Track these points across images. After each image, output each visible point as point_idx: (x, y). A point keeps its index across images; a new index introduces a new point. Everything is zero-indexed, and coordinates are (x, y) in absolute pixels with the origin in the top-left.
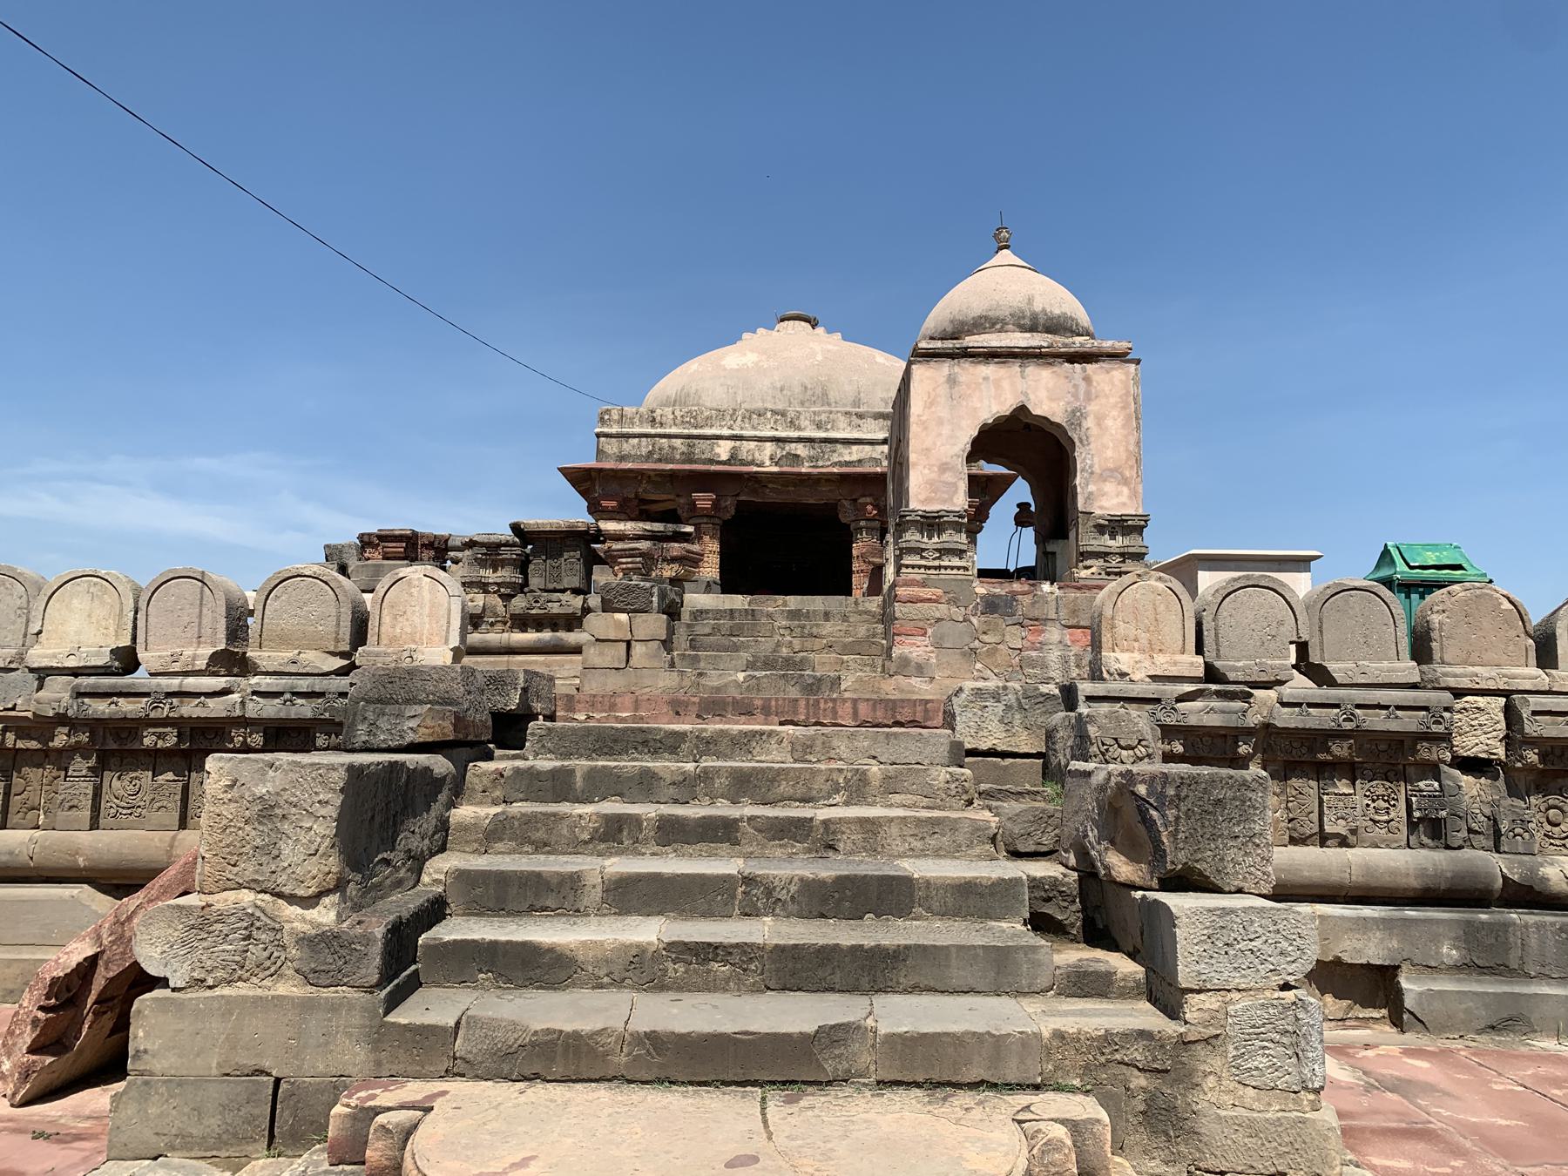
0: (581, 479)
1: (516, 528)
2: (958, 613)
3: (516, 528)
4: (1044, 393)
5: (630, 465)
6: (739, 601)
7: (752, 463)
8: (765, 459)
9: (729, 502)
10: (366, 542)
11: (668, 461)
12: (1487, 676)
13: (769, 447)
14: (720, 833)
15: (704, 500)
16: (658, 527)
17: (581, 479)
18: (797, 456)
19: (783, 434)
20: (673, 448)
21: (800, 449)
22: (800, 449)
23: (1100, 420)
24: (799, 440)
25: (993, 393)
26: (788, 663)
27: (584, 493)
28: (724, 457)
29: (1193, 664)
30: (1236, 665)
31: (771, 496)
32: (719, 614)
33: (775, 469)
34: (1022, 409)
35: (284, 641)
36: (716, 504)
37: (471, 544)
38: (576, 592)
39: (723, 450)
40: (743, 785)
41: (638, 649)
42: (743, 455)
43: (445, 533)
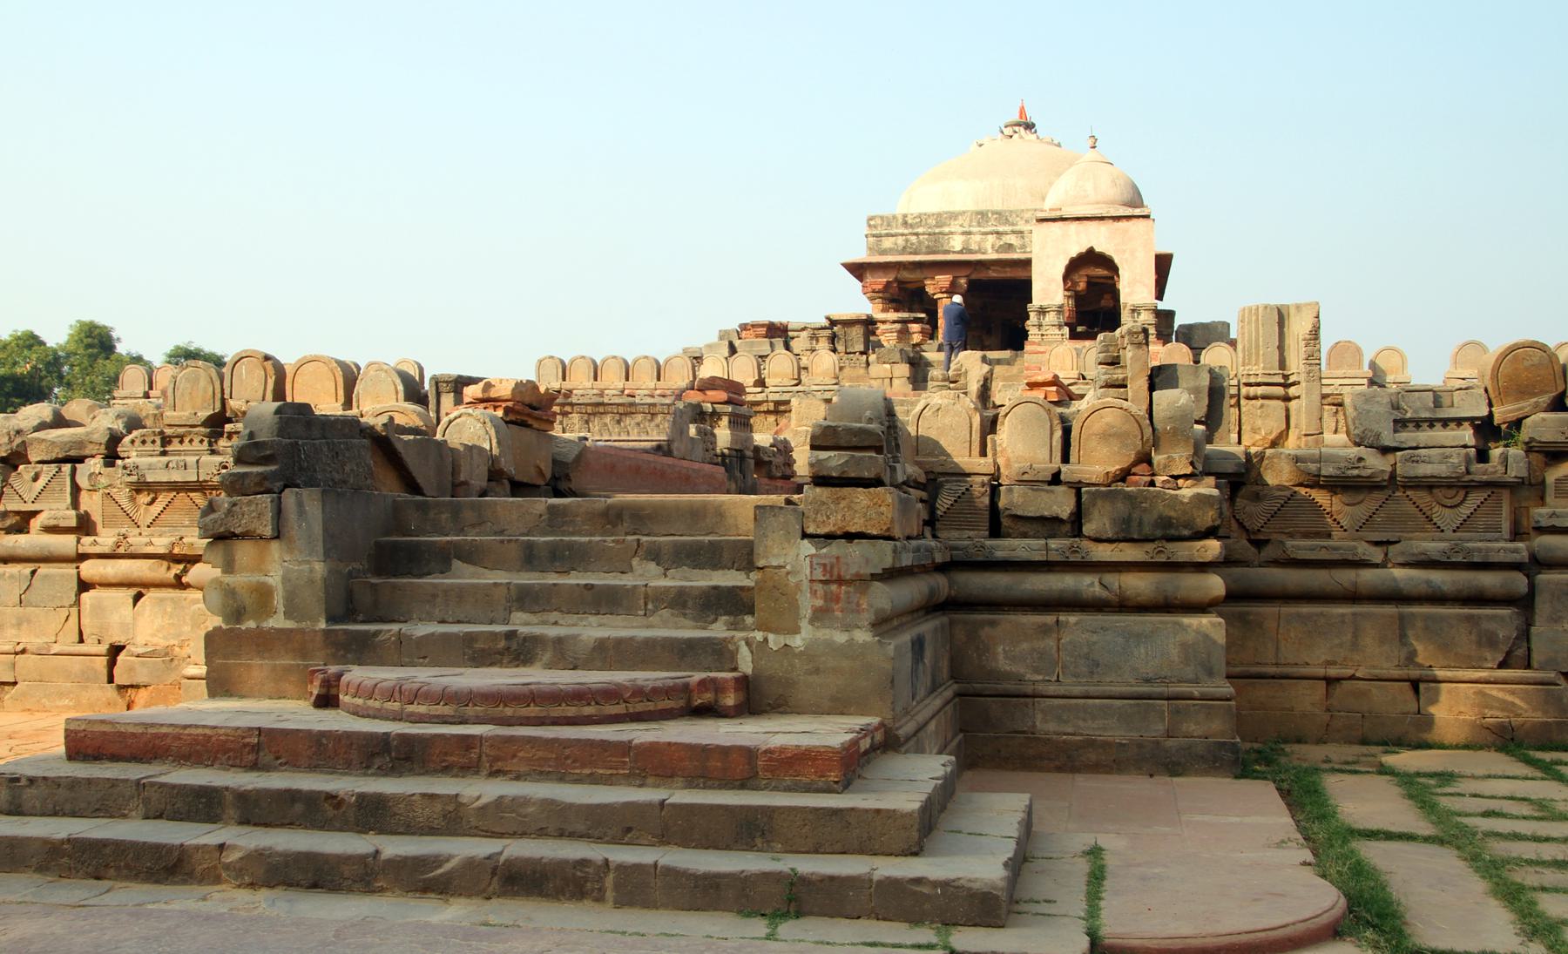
0: (858, 270)
3: (828, 318)
4: (1100, 239)
7: (979, 251)
8: (989, 251)
10: (744, 327)
11: (915, 253)
13: (991, 238)
15: (944, 280)
16: (905, 315)
18: (1010, 245)
19: (1001, 229)
20: (920, 242)
22: (1012, 239)
24: (1013, 232)
25: (1077, 240)
27: (860, 278)
28: (958, 248)
31: (993, 274)
33: (995, 256)
34: (1091, 251)
35: (776, 375)
37: (803, 329)
38: (862, 353)
39: (957, 243)
41: (895, 382)
42: (974, 247)
43: (784, 320)
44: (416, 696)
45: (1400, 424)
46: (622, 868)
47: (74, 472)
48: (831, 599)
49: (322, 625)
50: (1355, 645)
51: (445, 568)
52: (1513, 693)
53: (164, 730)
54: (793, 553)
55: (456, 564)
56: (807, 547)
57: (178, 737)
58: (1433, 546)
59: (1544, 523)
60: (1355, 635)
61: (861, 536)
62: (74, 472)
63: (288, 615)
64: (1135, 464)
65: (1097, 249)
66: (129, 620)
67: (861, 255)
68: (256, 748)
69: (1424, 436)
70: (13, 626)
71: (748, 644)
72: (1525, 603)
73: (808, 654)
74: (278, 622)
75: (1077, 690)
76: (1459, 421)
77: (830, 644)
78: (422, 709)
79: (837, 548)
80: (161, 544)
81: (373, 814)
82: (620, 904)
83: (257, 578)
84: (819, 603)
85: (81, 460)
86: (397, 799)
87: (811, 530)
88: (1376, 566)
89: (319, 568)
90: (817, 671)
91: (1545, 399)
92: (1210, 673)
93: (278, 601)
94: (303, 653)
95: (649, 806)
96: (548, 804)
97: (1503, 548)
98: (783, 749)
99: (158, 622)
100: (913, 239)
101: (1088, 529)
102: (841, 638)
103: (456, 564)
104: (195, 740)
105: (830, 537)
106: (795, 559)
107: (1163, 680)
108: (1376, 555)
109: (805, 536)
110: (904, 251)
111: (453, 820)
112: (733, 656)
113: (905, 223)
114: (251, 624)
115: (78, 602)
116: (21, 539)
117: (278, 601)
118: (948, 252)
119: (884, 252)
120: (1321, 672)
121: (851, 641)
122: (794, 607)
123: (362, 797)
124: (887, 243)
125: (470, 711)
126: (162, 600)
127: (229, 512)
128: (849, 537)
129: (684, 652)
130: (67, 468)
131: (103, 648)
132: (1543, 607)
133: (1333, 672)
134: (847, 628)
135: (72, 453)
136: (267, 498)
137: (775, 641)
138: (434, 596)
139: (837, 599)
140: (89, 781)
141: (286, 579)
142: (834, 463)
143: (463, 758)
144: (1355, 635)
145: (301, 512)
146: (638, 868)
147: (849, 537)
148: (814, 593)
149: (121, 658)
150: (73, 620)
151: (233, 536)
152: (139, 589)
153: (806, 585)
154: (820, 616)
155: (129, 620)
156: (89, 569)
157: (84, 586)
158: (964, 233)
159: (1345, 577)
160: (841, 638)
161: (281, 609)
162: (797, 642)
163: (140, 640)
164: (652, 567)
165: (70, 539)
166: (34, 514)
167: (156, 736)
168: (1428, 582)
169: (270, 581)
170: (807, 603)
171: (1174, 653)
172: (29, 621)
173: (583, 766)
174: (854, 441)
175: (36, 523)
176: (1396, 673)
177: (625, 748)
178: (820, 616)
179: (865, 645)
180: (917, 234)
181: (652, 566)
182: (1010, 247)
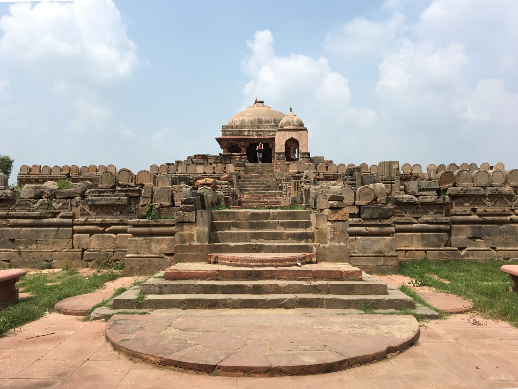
0: (219, 140)
1: (220, 154)
2: (283, 166)
3: (220, 154)
4: (294, 135)
5: (228, 137)
6: (253, 164)
9: (248, 144)
12: (322, 171)
13: (255, 133)
14: (258, 184)
15: (243, 143)
17: (219, 140)
21: (261, 133)
22: (261, 133)
23: (303, 139)
26: (261, 173)
27: (220, 143)
29: (297, 171)
30: (300, 171)
32: (250, 166)
33: (256, 137)
34: (292, 138)
36: (245, 144)
40: (259, 181)
44: (237, 260)
45: (420, 190)
46: (327, 299)
47: (71, 200)
48: (334, 235)
49: (207, 244)
50: (412, 242)
51: (229, 229)
52: (448, 253)
53: (193, 271)
54: (325, 225)
55: (232, 228)
56: (329, 224)
57: (197, 273)
58: (429, 218)
59: (453, 213)
60: (412, 240)
61: (341, 221)
62: (71, 200)
63: (198, 241)
64: (373, 201)
65: (294, 138)
66: (88, 242)
67: (220, 135)
68: (217, 275)
69: (425, 193)
70: (51, 244)
71: (315, 246)
72: (449, 232)
73: (330, 248)
74: (195, 243)
75: (361, 254)
76: (432, 190)
77: (335, 246)
78: (254, 264)
79: (336, 223)
80: (99, 220)
81: (257, 290)
82: (326, 308)
83: (189, 232)
84: (332, 236)
85: (73, 198)
86: (263, 285)
87: (330, 219)
88: (416, 223)
89: (207, 230)
90: (331, 252)
91: (451, 184)
92: (392, 250)
93: (195, 238)
94: (202, 251)
95: (325, 285)
96: (300, 285)
97: (443, 219)
98: (348, 271)
99: (97, 242)
100: (235, 132)
101: (363, 216)
102: (337, 244)
103: (232, 228)
104: (202, 274)
105: (334, 221)
106: (327, 226)
107: (381, 252)
108: (415, 221)
109: (328, 221)
110: (232, 135)
111: (277, 290)
112: (312, 249)
113: (232, 128)
114: (188, 244)
115: (72, 237)
116: (55, 220)
117: (195, 238)
118: (244, 136)
119: (227, 135)
120: (404, 248)
121: (339, 245)
122: (326, 238)
123: (254, 285)
124: (227, 133)
125: (266, 264)
126: (98, 236)
127: (183, 216)
128: (339, 221)
129: (300, 249)
130: (69, 200)
131: (80, 250)
132: (453, 232)
133: (407, 248)
134: (339, 242)
135: (71, 196)
136: (194, 212)
137: (321, 245)
138: (232, 236)
139: (336, 235)
140: (182, 285)
141: (197, 233)
142: (335, 204)
143: (271, 275)
144: (412, 240)
145: (202, 216)
146: (331, 299)
147: (339, 221)
148: (331, 234)
149: (85, 252)
150: (71, 242)
151: (184, 222)
152: (91, 233)
153: (329, 232)
154: (332, 239)
155: (88, 242)
156: (75, 227)
157: (74, 232)
158: (248, 131)
159: (409, 226)
160: (337, 244)
161: (196, 240)
162: (327, 246)
163: (91, 247)
164: (282, 228)
165: (70, 220)
166: (59, 213)
167: (191, 273)
168: (428, 227)
169: (193, 233)
170: (329, 236)
171: (383, 245)
172: (57, 243)
173: (301, 276)
174: (338, 199)
175: (60, 215)
176: (421, 248)
177: (310, 272)
178: (332, 239)
179: (343, 246)
180: (235, 131)
181: (282, 227)
182: (260, 135)
